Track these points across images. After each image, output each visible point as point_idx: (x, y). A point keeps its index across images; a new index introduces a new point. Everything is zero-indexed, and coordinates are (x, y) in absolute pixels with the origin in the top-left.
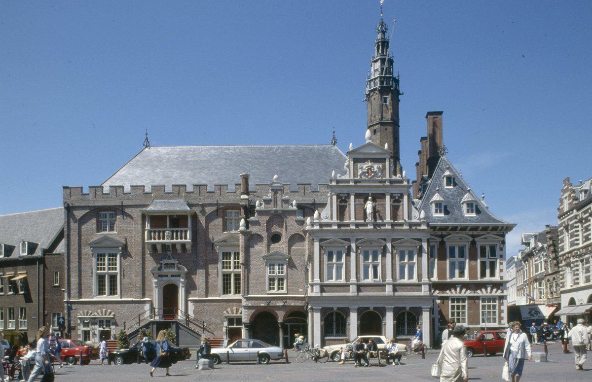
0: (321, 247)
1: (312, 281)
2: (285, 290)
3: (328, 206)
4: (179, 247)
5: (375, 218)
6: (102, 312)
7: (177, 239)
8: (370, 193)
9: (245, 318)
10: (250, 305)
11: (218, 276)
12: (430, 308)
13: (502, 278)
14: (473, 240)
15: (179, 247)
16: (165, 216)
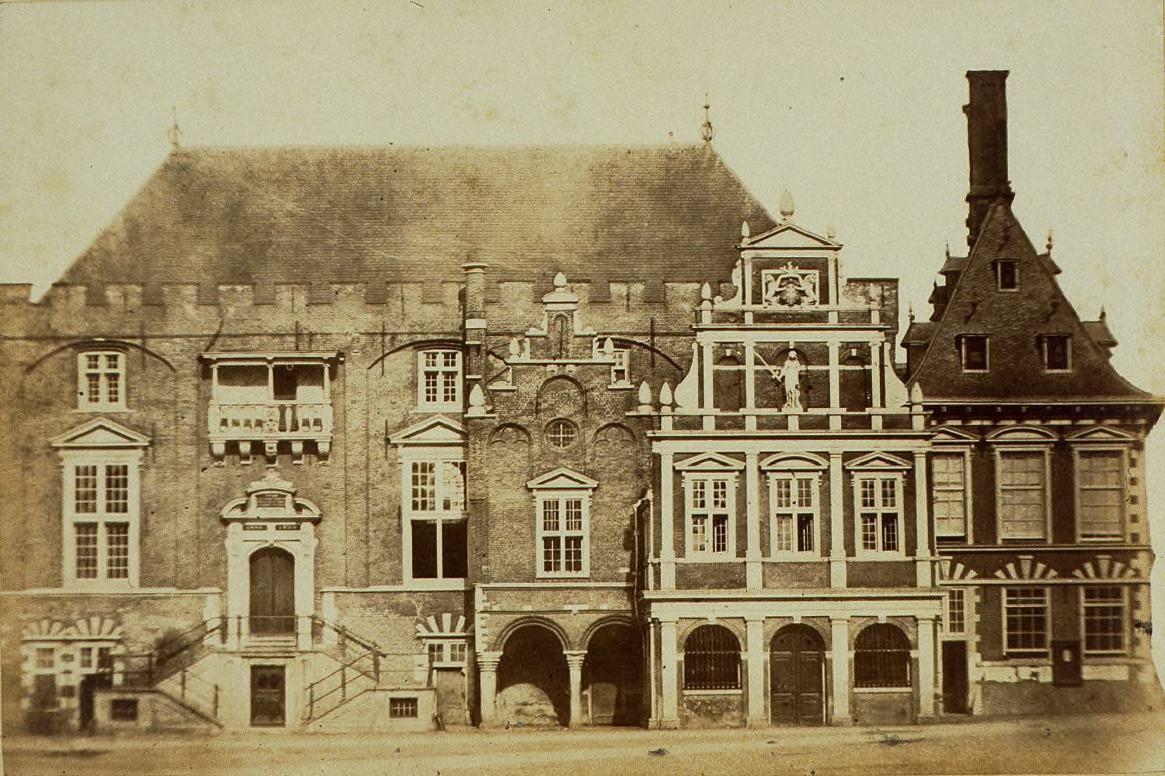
0: (677, 473)
1: (657, 555)
2: (585, 572)
3: (692, 376)
4: (297, 448)
5: (807, 404)
6: (89, 626)
7: (295, 428)
8: (793, 338)
9: (484, 642)
10: (495, 608)
11: (400, 530)
12: (937, 620)
13: (1135, 537)
14: (1061, 439)
15: (297, 448)
16: (264, 370)
